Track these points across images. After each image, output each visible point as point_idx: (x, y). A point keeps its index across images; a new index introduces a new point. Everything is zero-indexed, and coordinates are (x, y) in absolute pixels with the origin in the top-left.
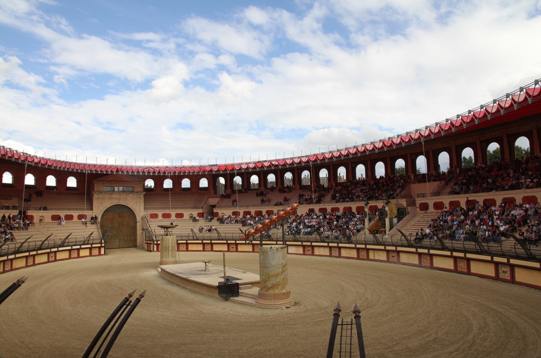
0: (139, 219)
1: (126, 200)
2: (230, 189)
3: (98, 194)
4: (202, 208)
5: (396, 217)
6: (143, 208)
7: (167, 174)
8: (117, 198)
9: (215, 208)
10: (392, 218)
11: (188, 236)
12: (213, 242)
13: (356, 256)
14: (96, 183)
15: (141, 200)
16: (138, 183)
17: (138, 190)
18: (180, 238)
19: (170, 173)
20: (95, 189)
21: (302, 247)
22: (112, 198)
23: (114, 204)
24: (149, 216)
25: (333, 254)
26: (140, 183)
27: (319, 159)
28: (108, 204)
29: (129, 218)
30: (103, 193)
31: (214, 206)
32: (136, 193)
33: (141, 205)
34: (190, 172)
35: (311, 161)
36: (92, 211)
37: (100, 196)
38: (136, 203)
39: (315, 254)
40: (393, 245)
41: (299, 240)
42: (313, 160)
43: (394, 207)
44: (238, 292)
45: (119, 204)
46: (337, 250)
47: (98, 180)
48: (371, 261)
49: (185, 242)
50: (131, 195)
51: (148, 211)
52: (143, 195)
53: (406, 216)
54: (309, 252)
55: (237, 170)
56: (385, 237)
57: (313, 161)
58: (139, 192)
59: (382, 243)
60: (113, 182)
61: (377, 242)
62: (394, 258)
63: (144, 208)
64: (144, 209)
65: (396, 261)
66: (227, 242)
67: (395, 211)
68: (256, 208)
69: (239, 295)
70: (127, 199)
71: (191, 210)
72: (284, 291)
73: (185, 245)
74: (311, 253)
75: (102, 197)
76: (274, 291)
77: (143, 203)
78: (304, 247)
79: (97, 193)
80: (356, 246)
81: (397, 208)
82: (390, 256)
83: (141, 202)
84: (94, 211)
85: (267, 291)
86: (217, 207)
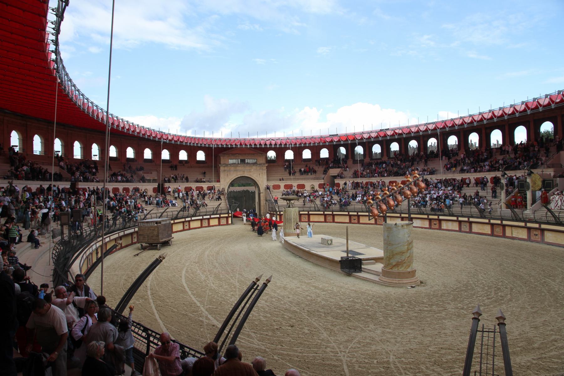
4: (323, 179)
5: (540, 190)
7: (288, 146)
8: (241, 170)
10: (536, 191)
11: (310, 208)
12: (334, 213)
13: (490, 233)
18: (302, 209)
19: (291, 144)
20: (222, 162)
21: (428, 220)
23: (239, 176)
25: (463, 230)
27: (447, 126)
28: (234, 176)
33: (264, 176)
34: (310, 143)
35: (438, 128)
36: (219, 183)
37: (226, 168)
38: (259, 174)
39: (442, 228)
40: (536, 222)
41: (425, 213)
42: (441, 127)
43: (538, 178)
44: (361, 268)
45: (244, 175)
46: (468, 224)
48: (507, 238)
49: (307, 213)
50: (254, 167)
51: (271, 182)
53: (553, 188)
54: (436, 226)
55: (359, 140)
56: (525, 212)
57: (441, 129)
59: (522, 219)
61: (515, 217)
62: (537, 237)
64: (267, 181)
65: (539, 240)
66: (349, 213)
67: (540, 183)
69: (361, 270)
71: (312, 181)
72: (409, 270)
74: (438, 227)
75: (228, 169)
76: (398, 269)
77: (266, 175)
78: (430, 220)
80: (489, 221)
81: (541, 180)
82: (532, 234)
85: (391, 269)
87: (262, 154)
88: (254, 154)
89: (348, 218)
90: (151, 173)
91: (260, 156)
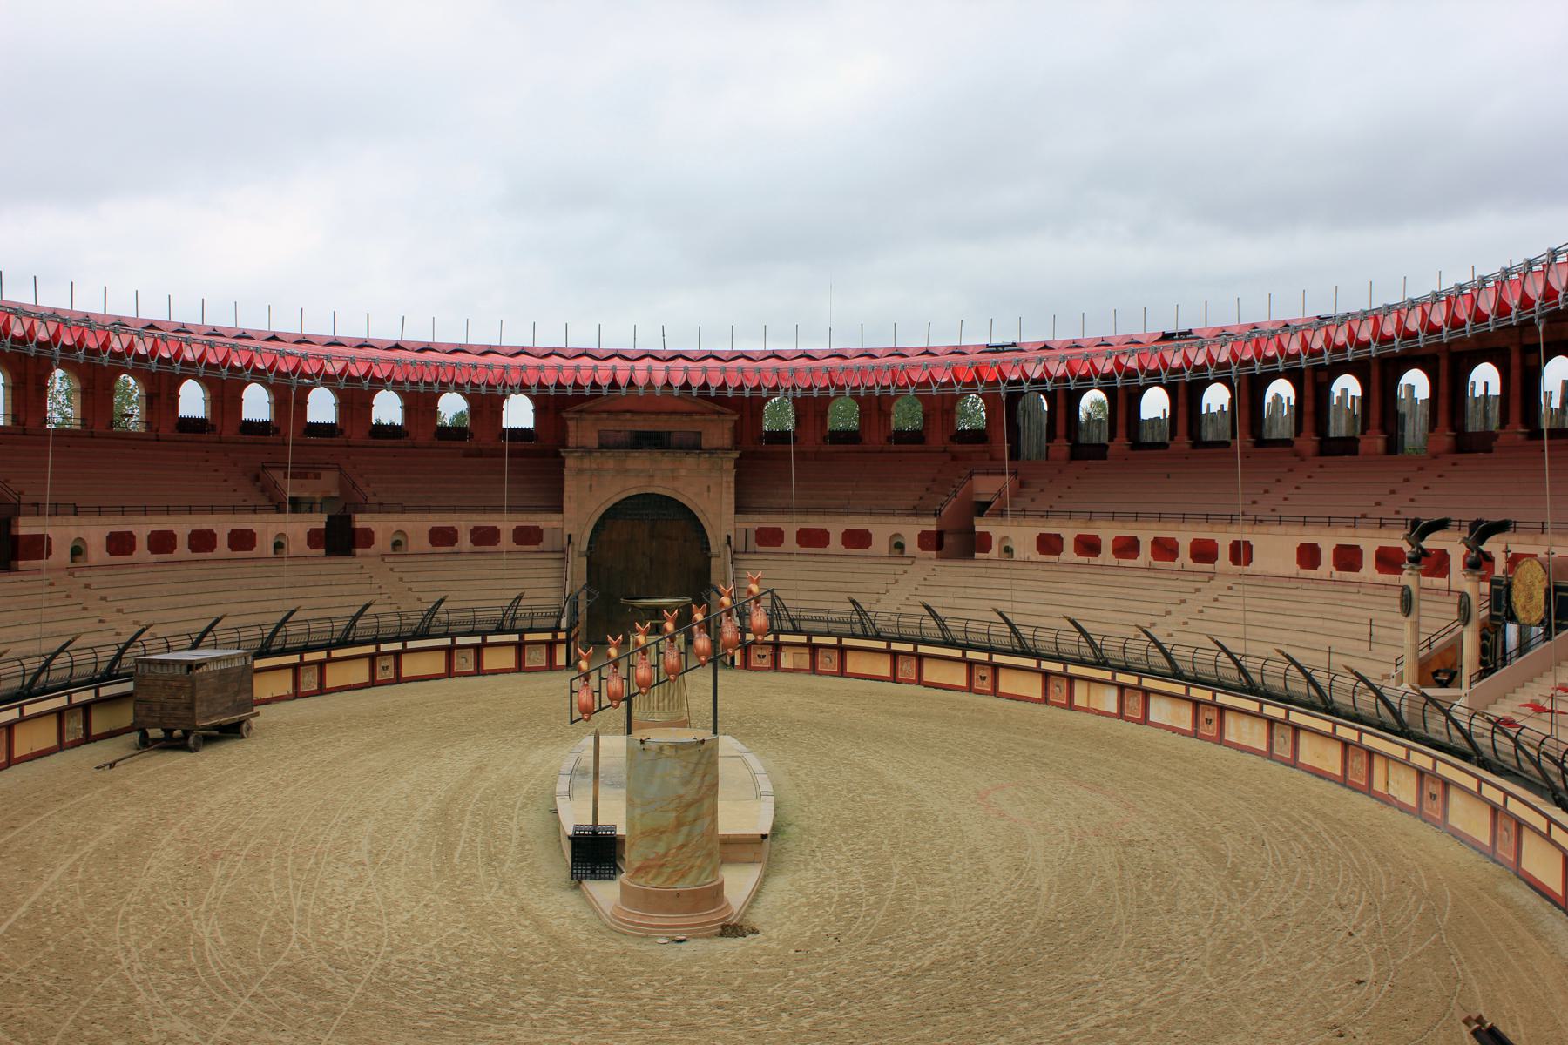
0: (716, 545)
1: (674, 478)
2: (1065, 442)
3: (578, 457)
4: (937, 514)
6: (733, 506)
9: (980, 514)
14: (573, 419)
15: (724, 479)
16: (716, 417)
17: (716, 442)
18: (822, 627)
20: (571, 441)
22: (627, 471)
23: (634, 492)
24: (752, 537)
26: (722, 417)
28: (613, 491)
29: (685, 541)
30: (595, 454)
31: (982, 508)
32: (707, 455)
33: (724, 495)
36: (559, 516)
37: (586, 464)
45: (650, 491)
47: (580, 411)
50: (690, 461)
51: (750, 517)
52: (733, 462)
58: (717, 449)
60: (628, 416)
63: (736, 507)
64: (736, 512)
68: (1119, 525)
70: (676, 475)
71: (896, 520)
73: (835, 655)
75: (594, 466)
77: (732, 490)
79: (576, 454)
83: (724, 485)
84: (566, 514)
86: (990, 515)
87: (718, 413)
88: (689, 414)
89: (962, 670)
90: (317, 477)
91: (712, 421)
